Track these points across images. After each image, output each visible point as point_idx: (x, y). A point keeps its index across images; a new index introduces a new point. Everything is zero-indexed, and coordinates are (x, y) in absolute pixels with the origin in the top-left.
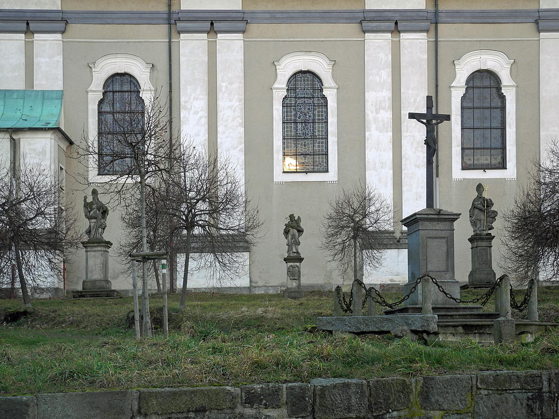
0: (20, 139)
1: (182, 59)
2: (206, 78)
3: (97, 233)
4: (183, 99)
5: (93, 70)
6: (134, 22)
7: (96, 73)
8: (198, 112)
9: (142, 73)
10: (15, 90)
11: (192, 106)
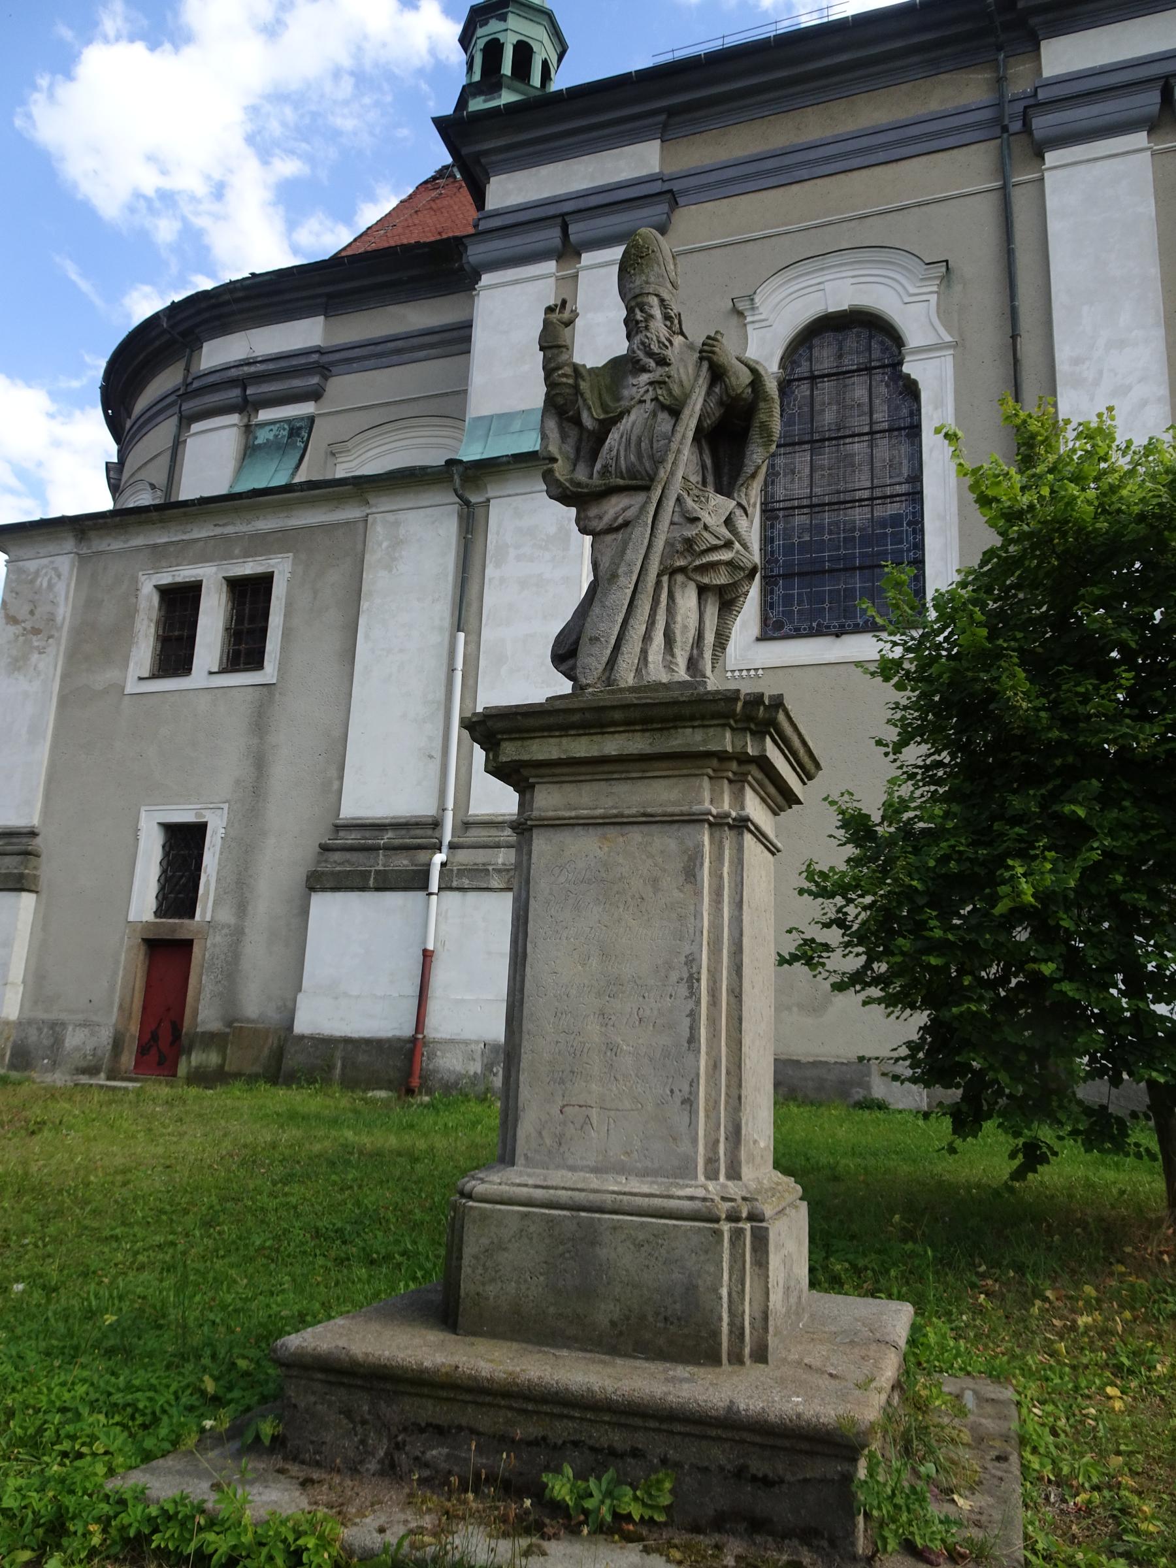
0: (488, 500)
1: (1054, 226)
2: (1154, 271)
3: (647, 638)
4: (1063, 353)
5: (749, 319)
6: (882, 156)
7: (757, 325)
8: (1129, 388)
9: (907, 299)
10: (517, 413)
11: (1101, 372)
